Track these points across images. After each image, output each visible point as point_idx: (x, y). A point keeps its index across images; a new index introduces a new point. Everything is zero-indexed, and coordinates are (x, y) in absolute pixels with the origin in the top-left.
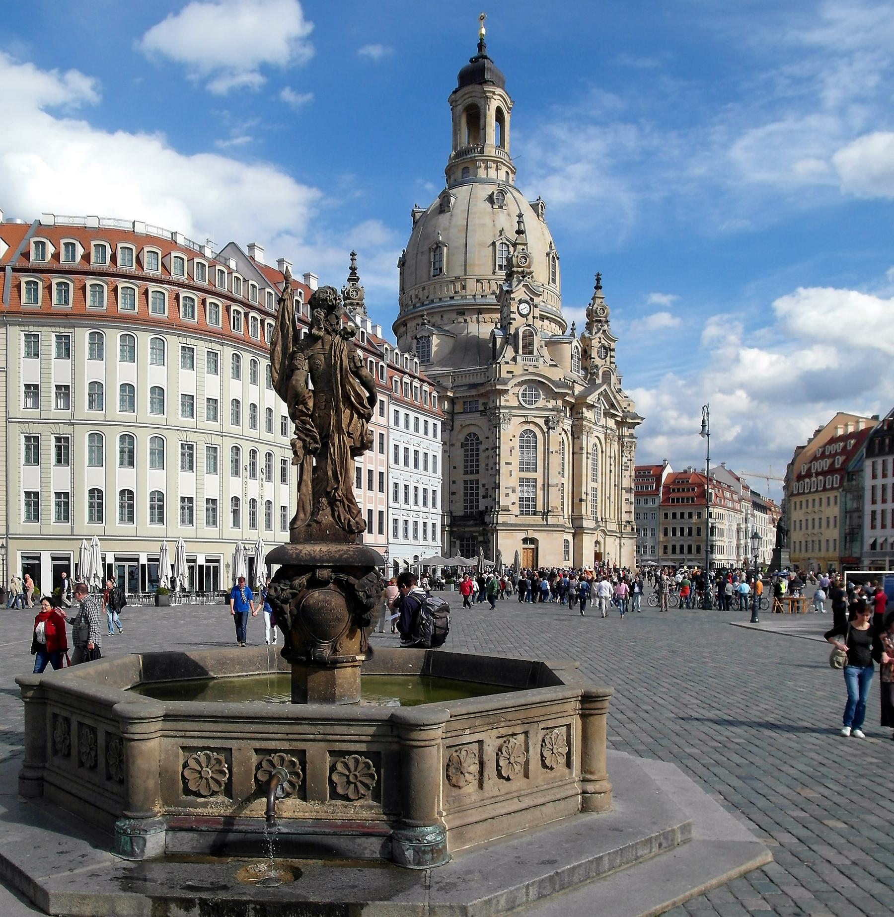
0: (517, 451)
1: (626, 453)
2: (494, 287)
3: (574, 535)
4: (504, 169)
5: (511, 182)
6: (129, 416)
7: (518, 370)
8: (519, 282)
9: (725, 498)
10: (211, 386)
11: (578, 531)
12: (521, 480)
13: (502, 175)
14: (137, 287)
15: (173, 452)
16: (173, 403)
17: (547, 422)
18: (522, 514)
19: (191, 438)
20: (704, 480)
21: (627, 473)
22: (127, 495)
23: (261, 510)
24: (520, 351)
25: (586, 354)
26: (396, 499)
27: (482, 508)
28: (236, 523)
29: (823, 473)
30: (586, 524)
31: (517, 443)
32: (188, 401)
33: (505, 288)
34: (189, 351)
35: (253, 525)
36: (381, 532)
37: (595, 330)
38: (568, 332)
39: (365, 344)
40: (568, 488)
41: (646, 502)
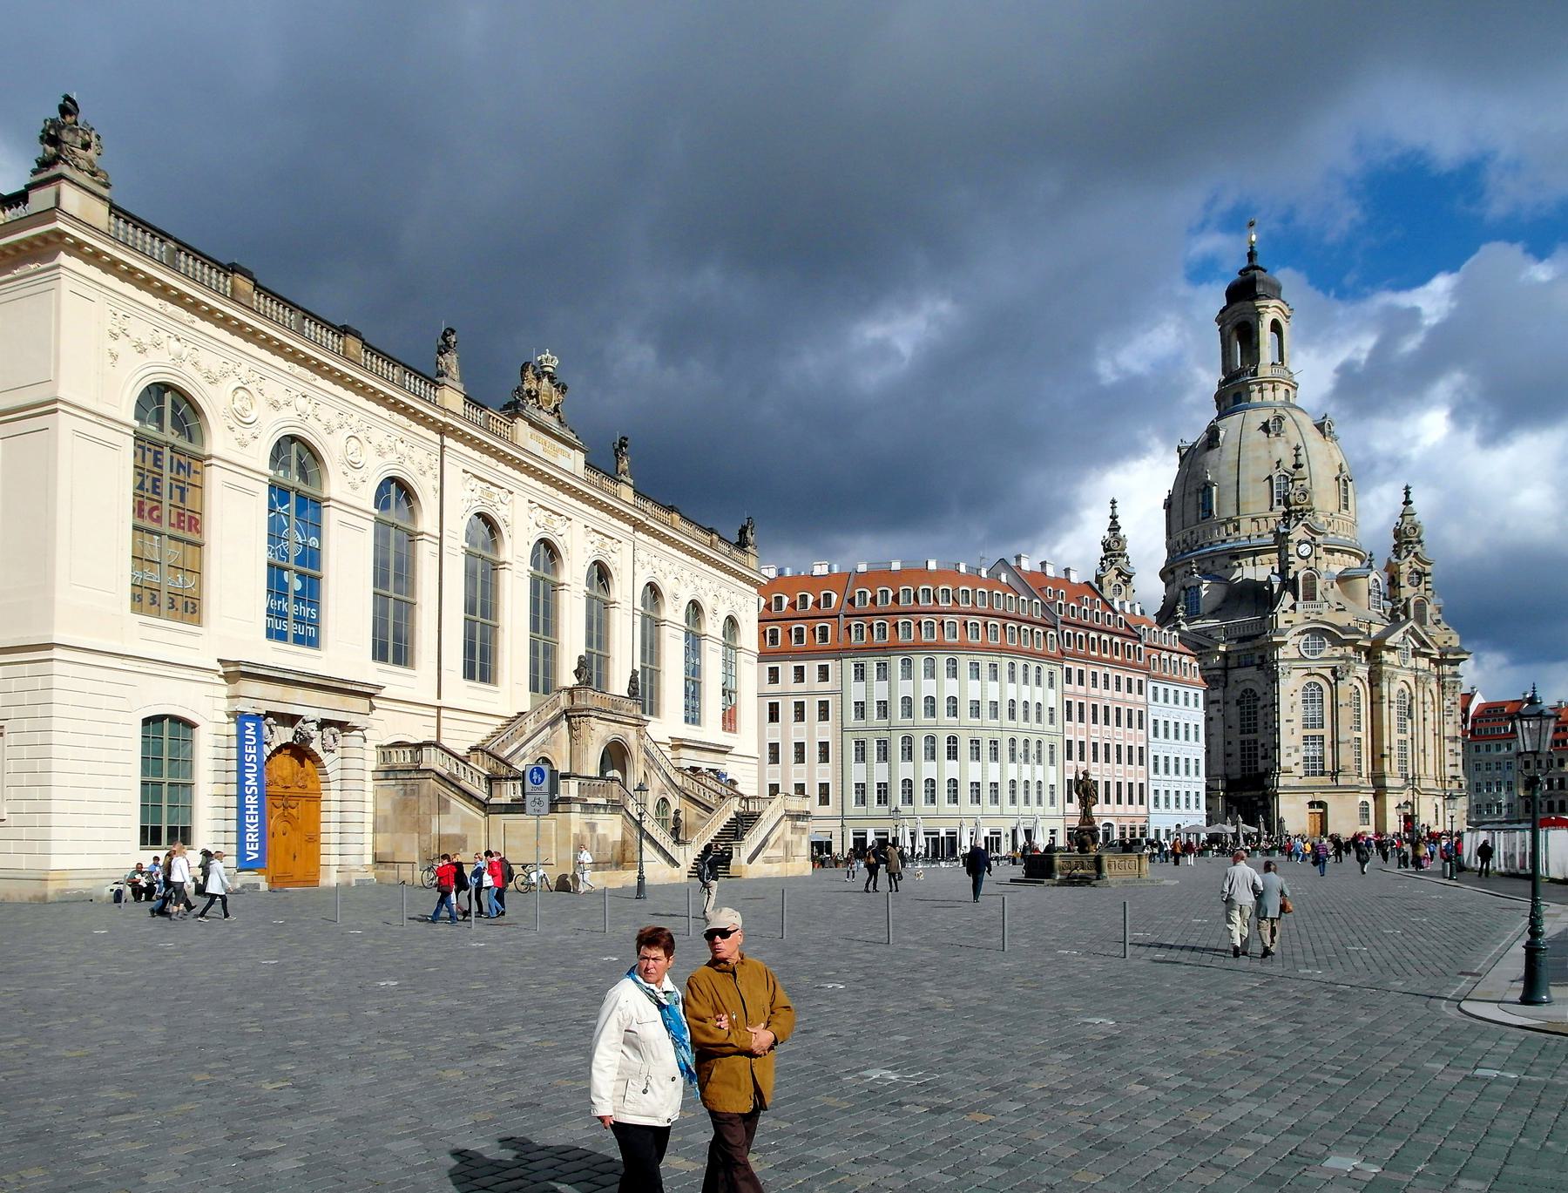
0: (1300, 707)
2: (1272, 525)
4: (1283, 387)
6: (931, 721)
7: (1298, 618)
8: (1298, 520)
10: (993, 691)
11: (1380, 791)
12: (1306, 738)
15: (964, 748)
16: (964, 708)
17: (1334, 672)
18: (1307, 774)
19: (978, 735)
22: (931, 782)
24: (1301, 597)
25: (1393, 582)
26: (1156, 771)
27: (1261, 769)
28: (1013, 801)
30: (1388, 783)
31: (1299, 697)
32: (976, 709)
33: (1282, 530)
34: (975, 668)
35: (1027, 802)
36: (1141, 802)
37: (1404, 553)
38: (1367, 563)
39: (1122, 629)
40: (1366, 742)
41: (1499, 748)
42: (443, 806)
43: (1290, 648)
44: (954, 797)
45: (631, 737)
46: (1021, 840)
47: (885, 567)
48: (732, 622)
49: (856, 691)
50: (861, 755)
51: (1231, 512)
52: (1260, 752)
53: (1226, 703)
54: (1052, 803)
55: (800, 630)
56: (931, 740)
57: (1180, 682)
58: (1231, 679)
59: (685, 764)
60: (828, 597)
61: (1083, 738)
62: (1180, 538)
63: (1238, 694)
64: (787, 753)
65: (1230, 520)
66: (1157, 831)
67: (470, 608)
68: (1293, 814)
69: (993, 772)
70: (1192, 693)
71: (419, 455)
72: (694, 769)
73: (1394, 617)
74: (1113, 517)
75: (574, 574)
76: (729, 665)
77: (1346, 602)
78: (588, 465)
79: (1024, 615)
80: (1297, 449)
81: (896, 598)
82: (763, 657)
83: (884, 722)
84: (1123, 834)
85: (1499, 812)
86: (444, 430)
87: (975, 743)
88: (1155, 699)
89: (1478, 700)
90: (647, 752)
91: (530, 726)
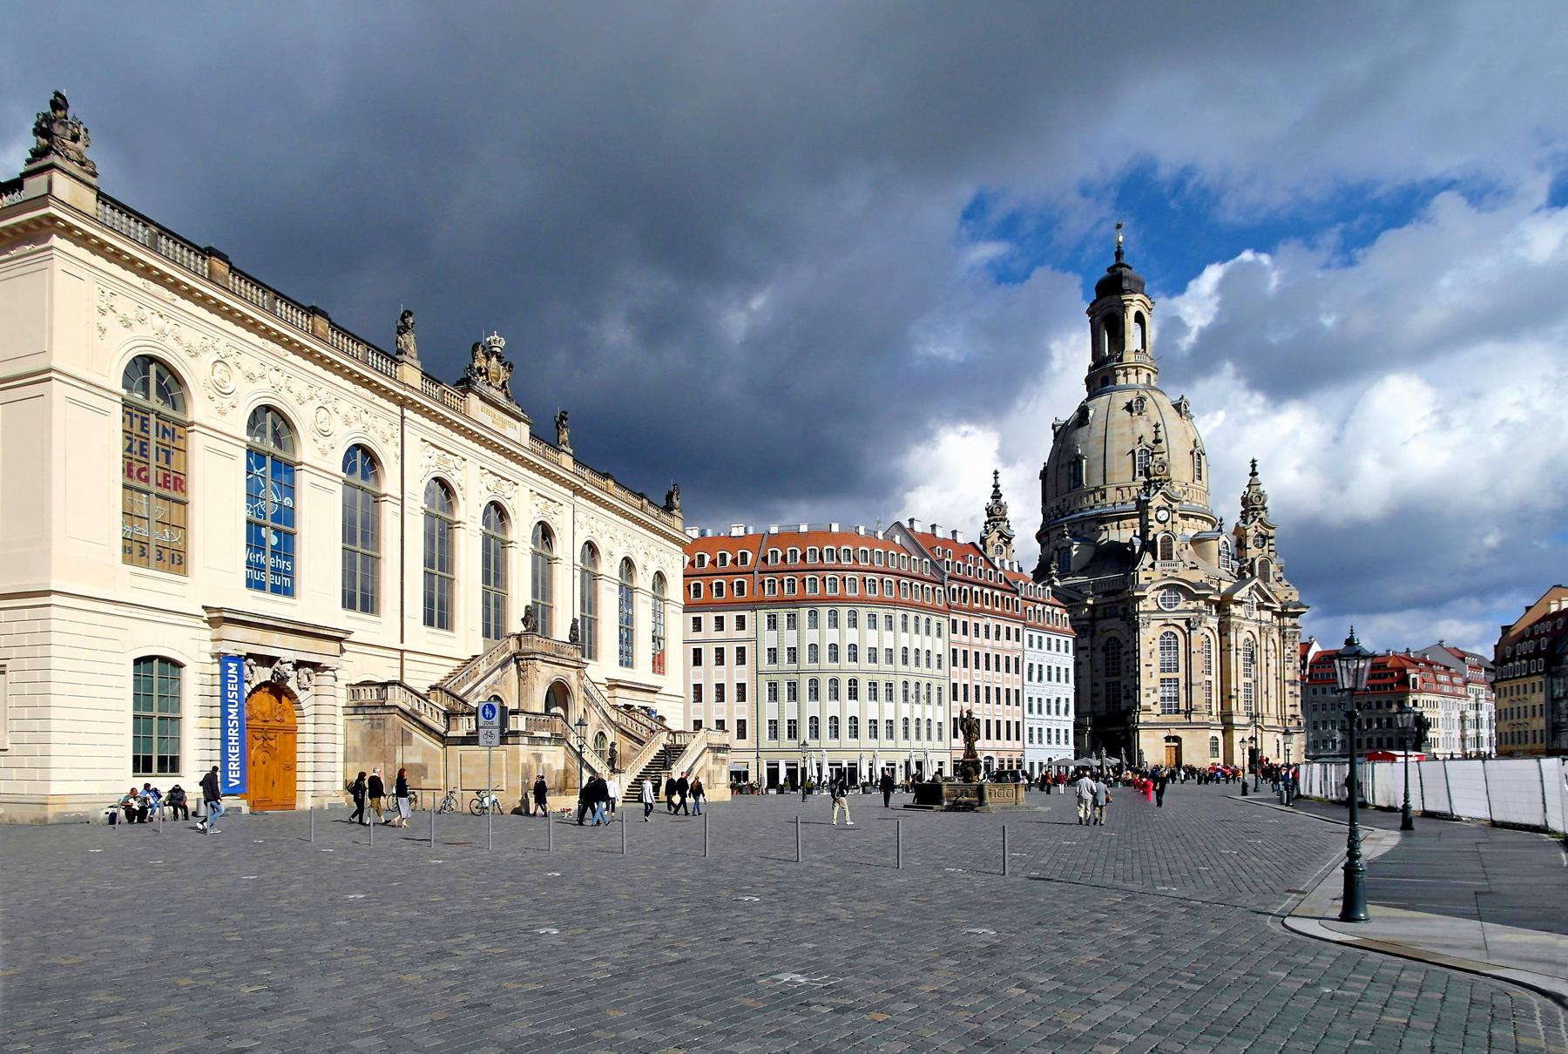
0: (1157, 654)
1: (1289, 644)
2: (1135, 493)
3: (1224, 732)
4: (1145, 372)
5: (1153, 383)
6: (835, 665)
7: (1156, 575)
8: (1157, 489)
9: (1438, 683)
11: (1228, 727)
12: (1163, 680)
13: (1143, 378)
14: (837, 576)
15: (863, 690)
16: (863, 654)
17: (1188, 623)
19: (875, 678)
20: (1406, 663)
21: (1291, 665)
22: (834, 719)
23: (924, 726)
25: (1241, 545)
26: (1030, 711)
28: (906, 737)
29: (1528, 657)
30: (1235, 720)
34: (873, 617)
35: (918, 738)
37: (1250, 519)
42: (406, 738)
43: (1149, 601)
44: (855, 733)
45: (572, 678)
46: (914, 769)
47: (794, 529)
48: (660, 576)
49: (769, 639)
50: (774, 696)
51: (1099, 482)
52: (1123, 693)
53: (1093, 649)
54: (940, 738)
55: (720, 585)
56: (834, 682)
57: (1053, 631)
58: (1098, 629)
59: (620, 702)
60: (744, 555)
61: (966, 682)
62: (1053, 505)
63: (1103, 642)
64: (709, 693)
65: (1097, 489)
66: (1032, 764)
67: (429, 562)
68: (1152, 749)
69: (889, 710)
70: (1063, 640)
71: (382, 425)
72: (628, 707)
73: (1241, 575)
74: (996, 486)
75: (521, 533)
76: (658, 614)
77: (1198, 561)
78: (532, 436)
79: (915, 572)
80: (1157, 426)
81: (804, 557)
82: (687, 608)
83: (794, 666)
84: (1002, 766)
85: (1334, 747)
86: (403, 403)
87: (873, 685)
88: (1031, 645)
89: (1316, 648)
90: (586, 691)
91: (483, 668)
